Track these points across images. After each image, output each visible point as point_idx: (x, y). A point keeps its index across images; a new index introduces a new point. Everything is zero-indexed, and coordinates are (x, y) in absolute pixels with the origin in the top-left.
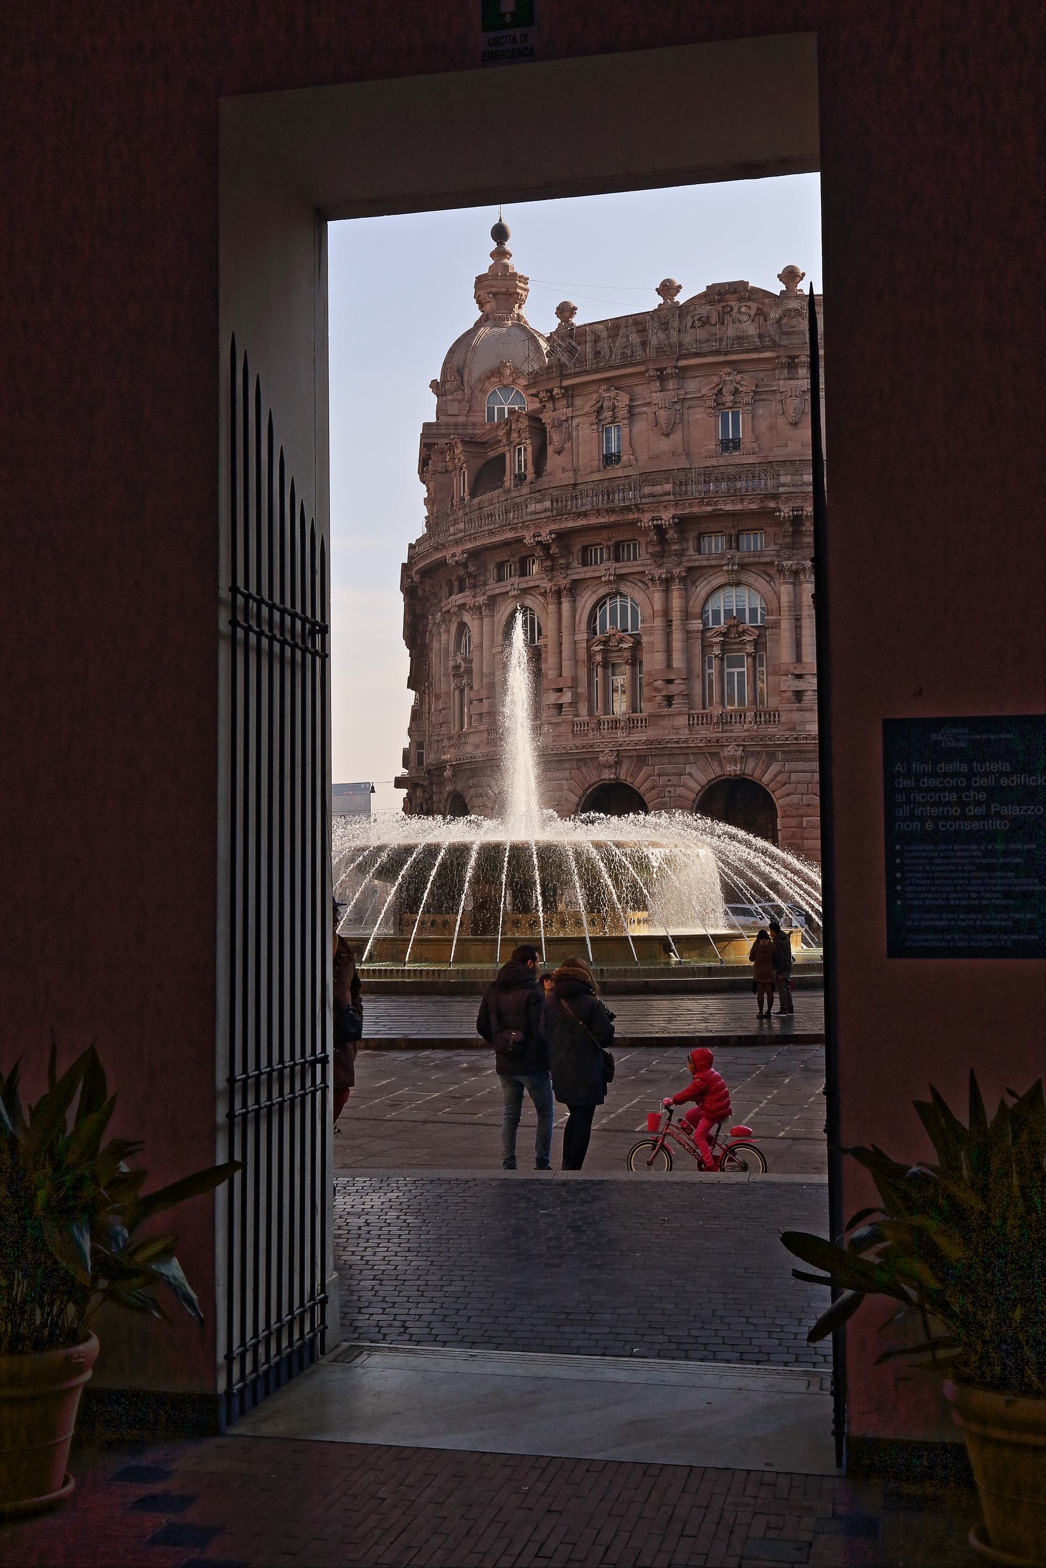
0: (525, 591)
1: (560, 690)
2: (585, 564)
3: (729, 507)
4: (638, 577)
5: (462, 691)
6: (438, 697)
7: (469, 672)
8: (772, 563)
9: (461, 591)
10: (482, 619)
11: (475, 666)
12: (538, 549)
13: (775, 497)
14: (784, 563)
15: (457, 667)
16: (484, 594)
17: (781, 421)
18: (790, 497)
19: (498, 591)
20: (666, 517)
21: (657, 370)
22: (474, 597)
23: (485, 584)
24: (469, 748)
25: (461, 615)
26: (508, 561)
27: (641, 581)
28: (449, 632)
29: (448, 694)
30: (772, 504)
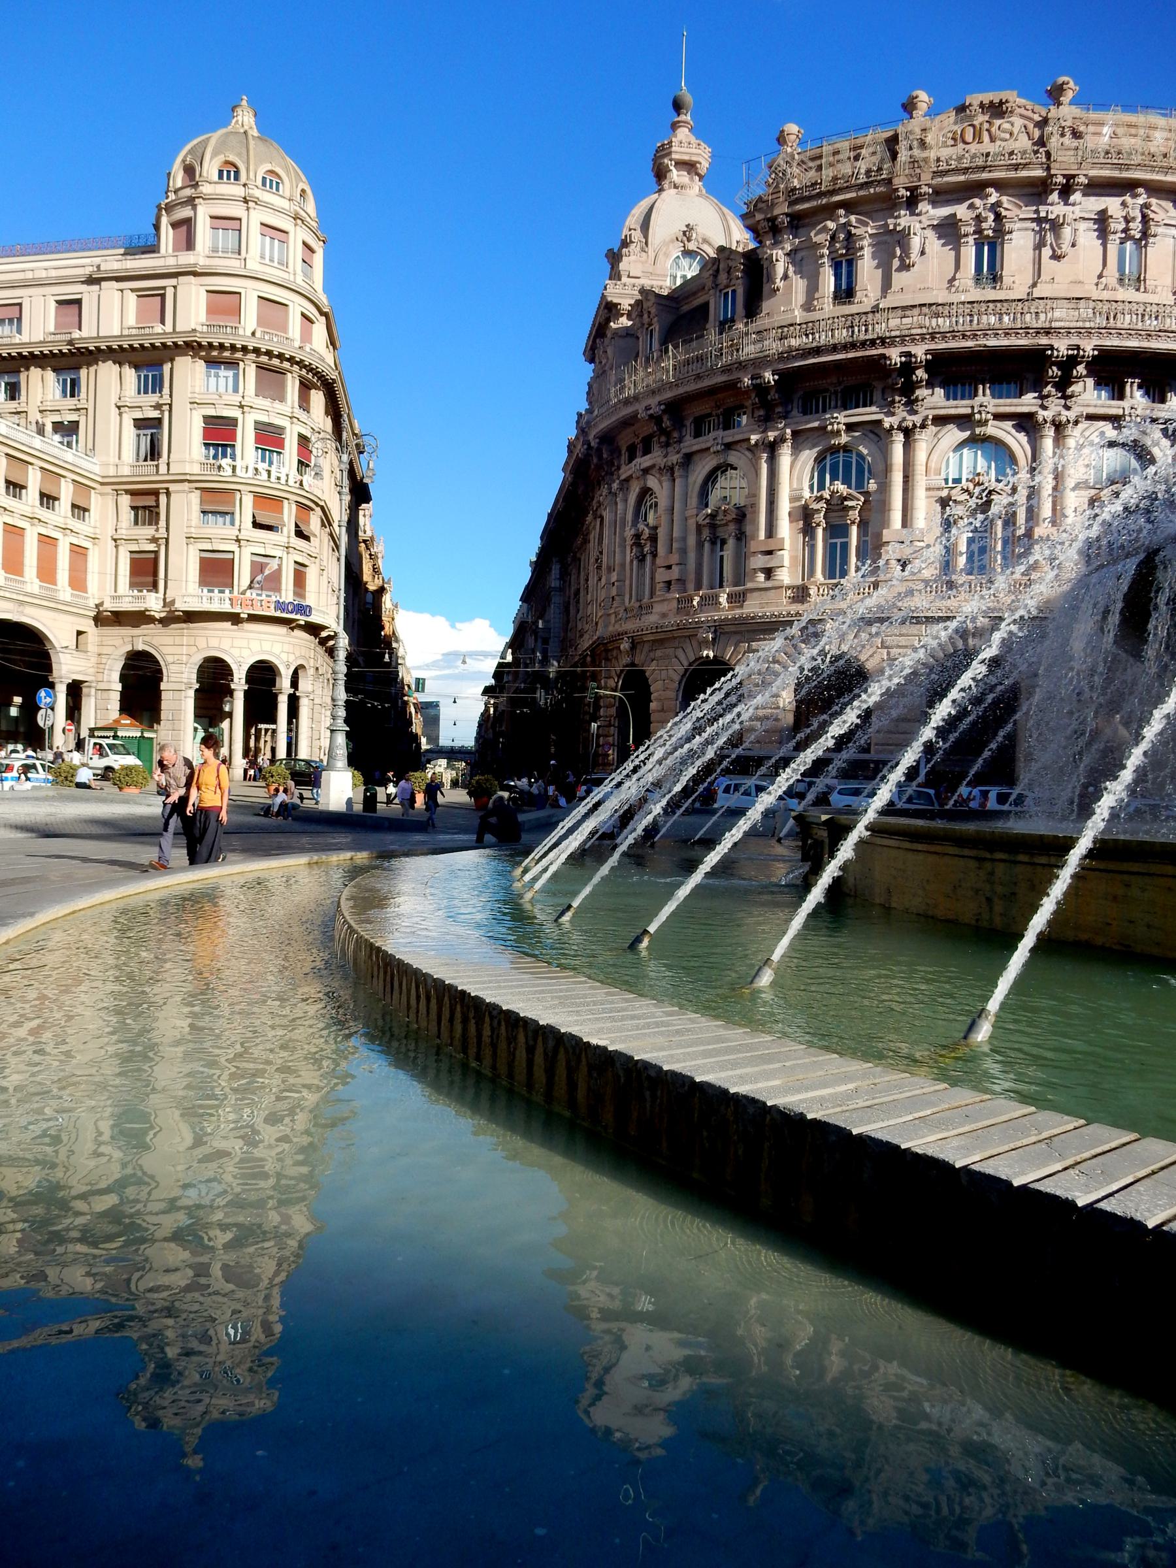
0: (729, 446)
1: (770, 553)
2: (805, 413)
3: (992, 342)
4: (869, 427)
5: (641, 559)
6: (610, 569)
7: (653, 539)
8: (1031, 416)
9: (647, 451)
10: (674, 480)
11: (662, 534)
12: (753, 395)
13: (1048, 332)
14: (1045, 413)
15: (637, 536)
16: (678, 452)
17: (1047, 252)
18: (1069, 331)
19: (695, 448)
20: (920, 351)
21: (907, 189)
22: (665, 456)
23: (680, 441)
24: (652, 619)
25: (645, 480)
26: (710, 415)
27: (871, 431)
28: (626, 501)
29: (623, 565)
30: (1044, 341)
